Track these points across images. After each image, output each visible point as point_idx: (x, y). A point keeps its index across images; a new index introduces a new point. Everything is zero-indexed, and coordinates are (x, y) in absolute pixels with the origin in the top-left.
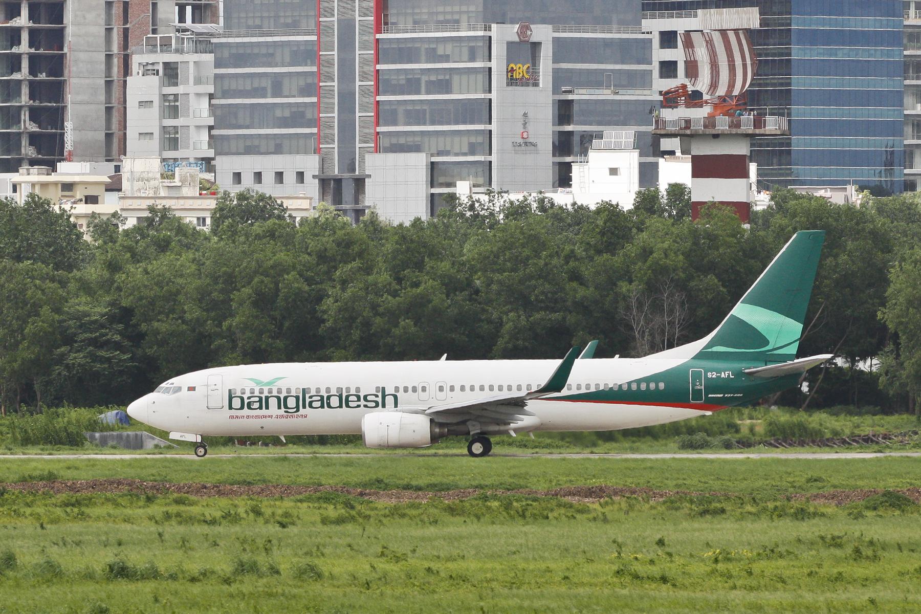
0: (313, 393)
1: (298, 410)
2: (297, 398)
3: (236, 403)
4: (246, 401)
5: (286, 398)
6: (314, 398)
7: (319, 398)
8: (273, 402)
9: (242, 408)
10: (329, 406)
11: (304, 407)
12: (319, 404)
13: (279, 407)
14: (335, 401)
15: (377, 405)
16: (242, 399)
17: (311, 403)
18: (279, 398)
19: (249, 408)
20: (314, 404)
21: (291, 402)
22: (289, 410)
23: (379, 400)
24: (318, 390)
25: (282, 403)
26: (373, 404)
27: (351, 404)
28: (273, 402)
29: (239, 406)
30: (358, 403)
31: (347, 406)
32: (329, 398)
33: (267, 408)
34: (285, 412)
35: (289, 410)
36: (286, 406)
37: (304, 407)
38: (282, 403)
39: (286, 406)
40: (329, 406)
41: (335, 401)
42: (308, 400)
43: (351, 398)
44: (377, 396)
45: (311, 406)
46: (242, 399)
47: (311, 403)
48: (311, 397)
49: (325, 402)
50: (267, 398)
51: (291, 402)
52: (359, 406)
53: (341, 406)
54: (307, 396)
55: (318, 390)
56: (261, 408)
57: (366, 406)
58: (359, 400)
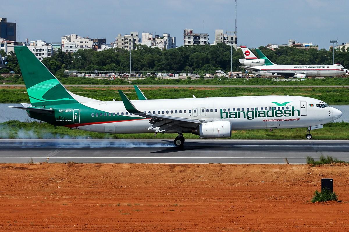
1: (253, 118)
2: (253, 112)
3: (224, 115)
4: (229, 114)
5: (248, 113)
6: (261, 112)
7: (263, 112)
8: (242, 114)
9: (227, 117)
10: (268, 116)
11: (256, 117)
12: (263, 115)
13: (245, 117)
14: (270, 114)
15: (290, 115)
16: (227, 113)
17: (259, 114)
18: (244, 113)
19: (230, 117)
20: (261, 115)
21: (250, 114)
22: (249, 118)
23: (291, 112)
26: (288, 115)
27: (278, 115)
28: (242, 114)
30: (282, 114)
31: (277, 116)
32: (268, 112)
33: (239, 117)
34: (248, 119)
35: (249, 118)
36: (248, 116)
37: (256, 117)
39: (248, 116)
40: (268, 116)
41: (270, 114)
42: (258, 113)
43: (278, 112)
44: (290, 111)
45: (259, 116)
46: (227, 113)
47: (259, 114)
48: (259, 112)
49: (266, 114)
50: (239, 113)
51: (250, 114)
52: (282, 116)
53: (273, 116)
54: (257, 111)
55: (262, 108)
56: (236, 117)
57: (285, 116)
58: (282, 113)
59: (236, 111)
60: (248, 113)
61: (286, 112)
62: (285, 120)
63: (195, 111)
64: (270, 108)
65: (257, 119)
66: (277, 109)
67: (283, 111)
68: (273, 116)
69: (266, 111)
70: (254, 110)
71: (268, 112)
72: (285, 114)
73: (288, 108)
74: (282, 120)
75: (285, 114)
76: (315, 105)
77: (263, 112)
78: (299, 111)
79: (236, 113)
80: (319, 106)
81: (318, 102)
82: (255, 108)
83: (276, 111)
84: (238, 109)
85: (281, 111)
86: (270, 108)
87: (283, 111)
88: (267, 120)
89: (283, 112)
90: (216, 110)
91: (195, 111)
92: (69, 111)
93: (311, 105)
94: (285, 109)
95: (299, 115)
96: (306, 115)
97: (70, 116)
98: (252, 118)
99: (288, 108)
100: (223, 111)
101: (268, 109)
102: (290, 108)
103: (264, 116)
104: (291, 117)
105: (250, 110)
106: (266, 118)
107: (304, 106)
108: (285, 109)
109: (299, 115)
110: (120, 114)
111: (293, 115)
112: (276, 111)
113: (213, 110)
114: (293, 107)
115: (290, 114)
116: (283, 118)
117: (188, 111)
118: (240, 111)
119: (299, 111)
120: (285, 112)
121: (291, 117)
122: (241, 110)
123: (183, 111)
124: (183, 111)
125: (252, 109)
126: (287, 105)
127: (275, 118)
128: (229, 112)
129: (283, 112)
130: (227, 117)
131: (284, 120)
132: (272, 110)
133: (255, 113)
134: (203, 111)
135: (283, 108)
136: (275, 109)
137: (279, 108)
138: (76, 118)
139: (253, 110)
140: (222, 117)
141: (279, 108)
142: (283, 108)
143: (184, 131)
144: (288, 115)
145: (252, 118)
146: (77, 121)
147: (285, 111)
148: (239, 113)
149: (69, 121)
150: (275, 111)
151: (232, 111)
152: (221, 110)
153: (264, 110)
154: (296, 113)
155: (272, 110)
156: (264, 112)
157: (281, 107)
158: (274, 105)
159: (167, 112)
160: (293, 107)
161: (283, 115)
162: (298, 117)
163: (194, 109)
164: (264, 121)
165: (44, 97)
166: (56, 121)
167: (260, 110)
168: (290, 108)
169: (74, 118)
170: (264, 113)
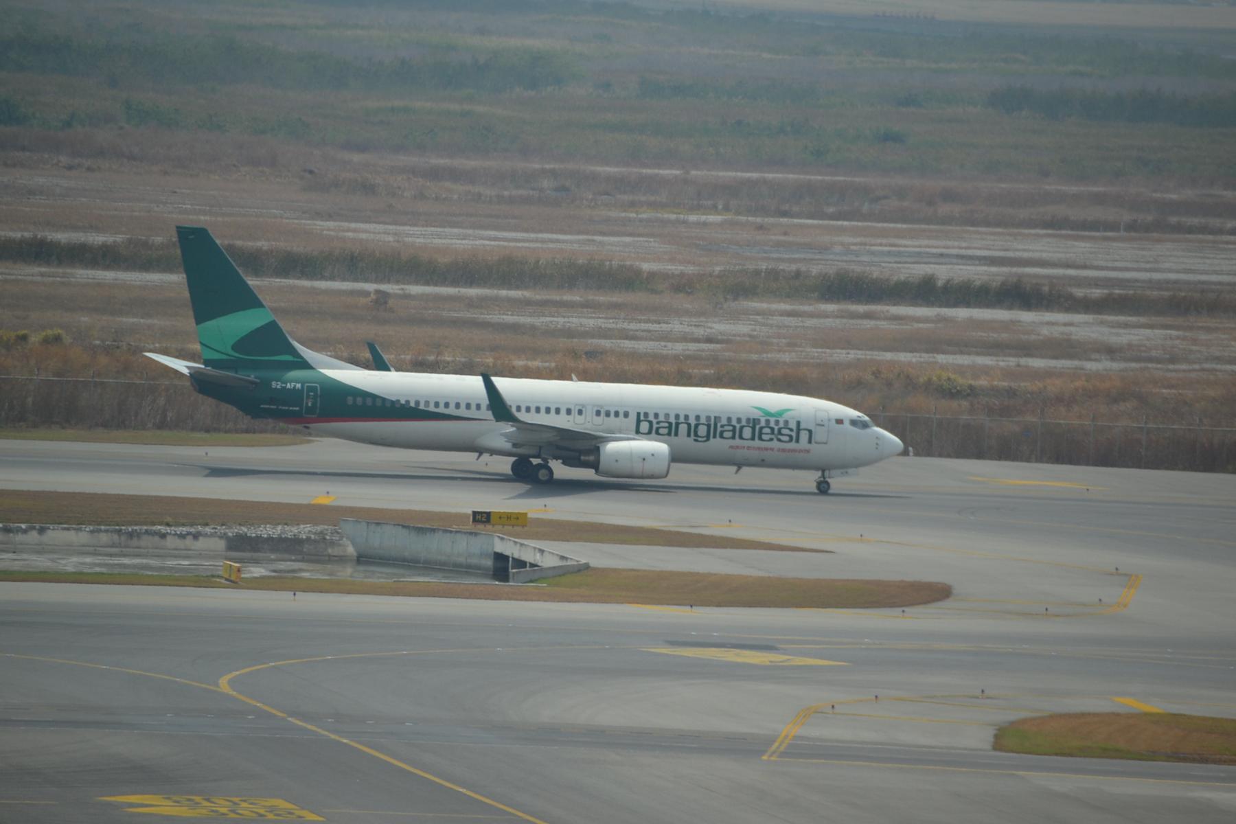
2: (709, 426)
3: (644, 426)
4: (655, 426)
5: (697, 426)
6: (726, 428)
7: (731, 428)
8: (683, 428)
9: (650, 432)
10: (741, 437)
13: (689, 435)
14: (747, 432)
15: (791, 440)
16: (651, 423)
18: (689, 425)
19: (657, 433)
20: (726, 434)
21: (702, 430)
22: (700, 439)
23: (794, 434)
24: (729, 419)
25: (692, 431)
26: (786, 438)
27: (764, 437)
28: (683, 428)
29: (646, 431)
30: (773, 436)
31: (760, 439)
32: (742, 428)
33: (676, 434)
34: (696, 440)
35: (700, 439)
36: (696, 435)
37: (715, 437)
38: (692, 431)
39: (696, 435)
40: (741, 437)
41: (747, 432)
42: (719, 429)
44: (791, 430)
45: (721, 436)
46: (651, 423)
48: (722, 426)
49: (736, 433)
50: (677, 424)
51: (702, 430)
52: (771, 440)
53: (753, 438)
54: (719, 425)
55: (729, 419)
56: (669, 434)
57: (779, 440)
58: (773, 433)
59: (672, 420)
60: (697, 426)
62: (779, 450)
66: (763, 423)
67: (776, 428)
68: (753, 438)
69: (738, 426)
71: (742, 428)
73: (786, 422)
76: (847, 424)
77: (731, 428)
79: (670, 424)
80: (854, 422)
81: (854, 413)
82: (715, 417)
83: (761, 428)
84: (677, 416)
85: (772, 429)
86: (748, 420)
87: (776, 428)
88: (737, 447)
89: (776, 432)
90: (626, 415)
91: (580, 412)
92: (295, 386)
93: (840, 421)
94: (781, 425)
95: (810, 442)
96: (824, 441)
97: (294, 396)
98: (705, 439)
100: (642, 418)
101: (744, 423)
102: (793, 425)
103: (733, 437)
105: (703, 420)
106: (737, 442)
108: (781, 425)
110: (412, 404)
111: (797, 441)
112: (761, 428)
113: (701, 417)
114: (798, 423)
115: (791, 437)
118: (680, 421)
119: (810, 432)
120: (780, 433)
121: (793, 445)
122: (682, 419)
125: (708, 418)
126: (785, 416)
127: (757, 443)
128: (654, 421)
129: (776, 432)
130: (650, 432)
132: (751, 425)
134: (598, 413)
135: (777, 422)
136: (759, 424)
137: (768, 421)
138: (310, 405)
140: (638, 432)
141: (768, 421)
142: (777, 422)
144: (786, 438)
145: (705, 439)
146: (310, 410)
147: (780, 430)
148: (677, 424)
149: (295, 409)
150: (757, 427)
151: (661, 418)
152: (639, 414)
154: (804, 436)
155: (751, 425)
156: (734, 427)
157: (772, 420)
158: (756, 414)
159: (569, 412)
160: (798, 423)
161: (775, 439)
162: (808, 446)
163: (578, 408)
164: (731, 447)
166: (262, 406)
167: (724, 422)
168: (793, 425)
169: (307, 403)
170: (734, 431)
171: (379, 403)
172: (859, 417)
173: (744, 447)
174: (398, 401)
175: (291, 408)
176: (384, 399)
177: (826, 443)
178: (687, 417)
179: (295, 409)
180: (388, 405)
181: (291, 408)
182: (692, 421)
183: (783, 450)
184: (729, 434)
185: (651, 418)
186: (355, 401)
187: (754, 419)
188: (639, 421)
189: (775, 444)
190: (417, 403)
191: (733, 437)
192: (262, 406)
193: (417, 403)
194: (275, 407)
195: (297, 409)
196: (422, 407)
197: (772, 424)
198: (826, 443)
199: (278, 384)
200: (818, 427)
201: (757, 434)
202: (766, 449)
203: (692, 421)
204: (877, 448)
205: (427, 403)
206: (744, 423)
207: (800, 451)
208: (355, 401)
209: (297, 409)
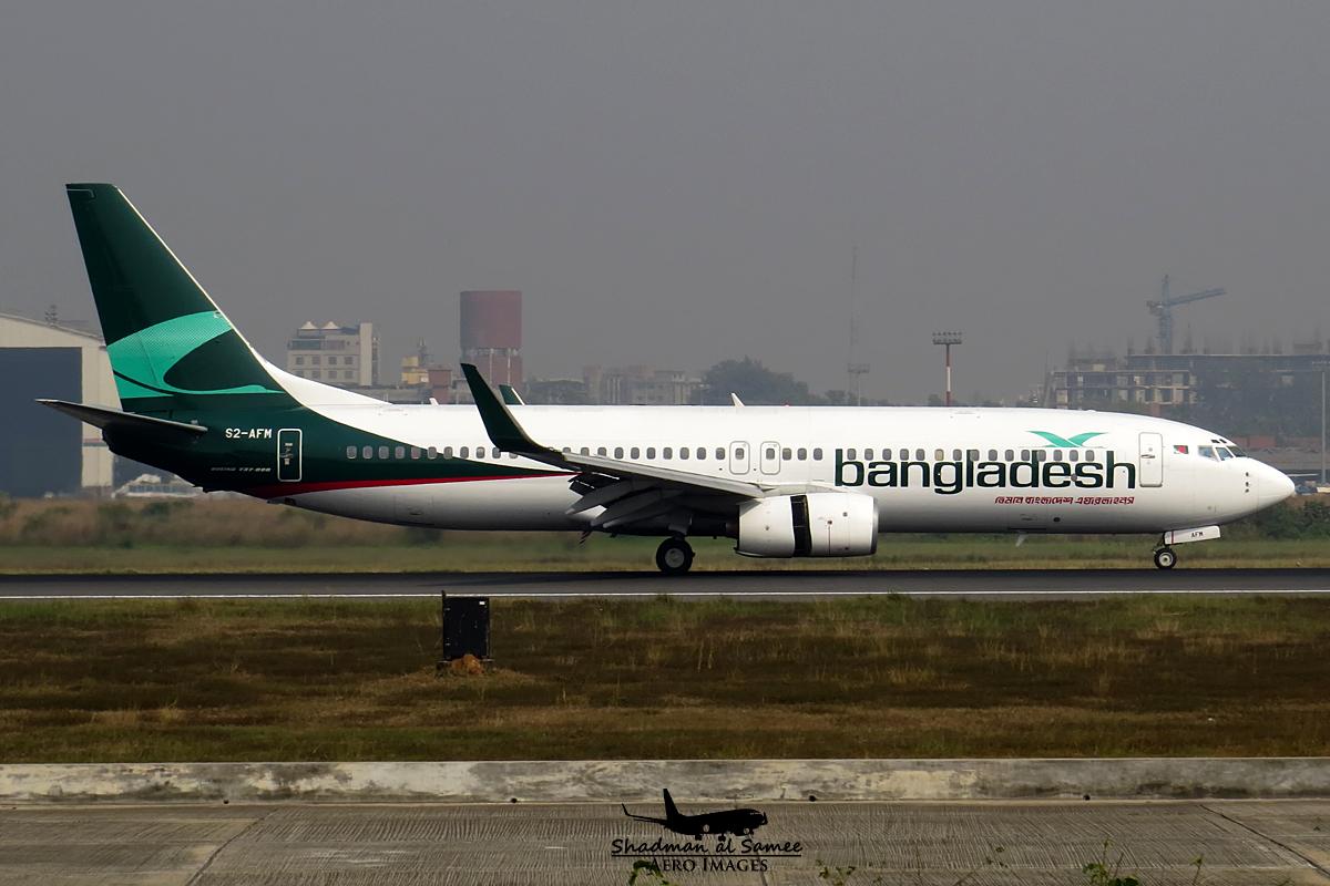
0: (984, 458)
1: (959, 489)
2: (958, 467)
3: (850, 473)
4: (867, 471)
5: (938, 467)
6: (988, 468)
7: (996, 468)
8: (915, 473)
9: (859, 482)
10: (1014, 483)
11: (970, 483)
13: (926, 483)
14: (1024, 474)
15: (1099, 483)
16: (860, 467)
17: (981, 476)
18: (926, 467)
19: (872, 482)
20: (987, 479)
21: (948, 474)
22: (944, 489)
23: (1103, 473)
24: (993, 454)
25: (931, 476)
26: (1093, 481)
27: (1053, 479)
28: (915, 473)
30: (1069, 479)
31: (1047, 483)
32: (1014, 467)
33: (904, 483)
34: (938, 491)
35: (944, 489)
37: (970, 483)
39: (938, 481)
40: (1014, 483)
41: (1024, 474)
42: (976, 471)
43: (1053, 470)
44: (1099, 467)
45: (981, 483)
46: (860, 467)
47: (981, 476)
48: (982, 466)
49: (1007, 475)
50: (905, 467)
51: (948, 474)
52: (1067, 484)
53: (1034, 483)
54: (976, 464)
55: (993, 454)
56: (893, 483)
57: (1079, 484)
60: (938, 467)
61: (1086, 470)
63: (740, 453)
64: (1025, 454)
65: (973, 495)
68: (1034, 483)
70: (964, 461)
71: (1014, 467)
72: (1079, 479)
73: (1090, 454)
74: (1067, 500)
75: (1079, 479)
76: (1193, 450)
77: (996, 468)
78: (1131, 469)
79: (893, 466)
81: (1204, 437)
82: (968, 451)
83: (1047, 467)
84: (904, 454)
85: (1067, 468)
86: (1025, 454)
88: (1010, 499)
89: (1073, 471)
90: (818, 455)
91: (740, 453)
93: (1184, 449)
95: (1132, 485)
96: (1159, 483)
97: (263, 452)
98: (954, 487)
99: (1090, 454)
100: (845, 459)
101: (1018, 458)
102: (1101, 459)
103: (1002, 483)
104: (1103, 491)
105: (949, 458)
106: (1009, 490)
107: (1151, 450)
109: (1132, 485)
110: (456, 454)
111: (1110, 484)
112: (1047, 467)
114: (1110, 455)
115: (1099, 478)
116: (1073, 491)
117: (711, 454)
118: (909, 461)
121: (1103, 491)
122: (912, 458)
123: (810, 454)
124: (810, 454)
125: (957, 454)
126: (1090, 444)
127: (1042, 491)
128: (866, 464)
129: (1073, 471)
130: (859, 482)
131: (1075, 499)
132: (1030, 462)
133: (968, 471)
134: (770, 454)
135: (1074, 456)
137: (1058, 454)
138: (287, 463)
139: (960, 459)
140: (839, 481)
141: (1058, 454)
142: (1074, 456)
143: (819, 533)
144: (1093, 481)
145: (954, 487)
146: (290, 471)
147: (1079, 468)
148: (905, 467)
151: (878, 457)
152: (839, 453)
153: (1001, 459)
154: (1121, 475)
155: (1030, 462)
160: (1110, 455)
161: (1073, 483)
162: (1130, 493)
164: (1000, 500)
165: (170, 377)
166: (213, 469)
167: (984, 458)
171: (400, 454)
172: (1214, 441)
173: (1022, 499)
174: (433, 449)
175: (258, 470)
176: (408, 447)
177: (1160, 486)
178: (921, 454)
179: (263, 470)
180: (415, 457)
181: (258, 470)
182: (932, 462)
183: (1088, 500)
184: (886, 478)
185: (860, 458)
186: (360, 453)
187: (1034, 452)
188: (839, 466)
189: (1073, 491)
190: (465, 451)
191: (1002, 483)
192: (213, 469)
193: (465, 451)
194: (234, 469)
195: (269, 470)
196: (472, 457)
197: (1066, 459)
198: (1160, 486)
199: (234, 433)
200: (1144, 460)
201: (1040, 475)
202: (1059, 500)
203: (932, 462)
204: (1247, 491)
205: (481, 454)
206: (1018, 458)
207: (1117, 500)
208: (360, 453)
209: (269, 470)
